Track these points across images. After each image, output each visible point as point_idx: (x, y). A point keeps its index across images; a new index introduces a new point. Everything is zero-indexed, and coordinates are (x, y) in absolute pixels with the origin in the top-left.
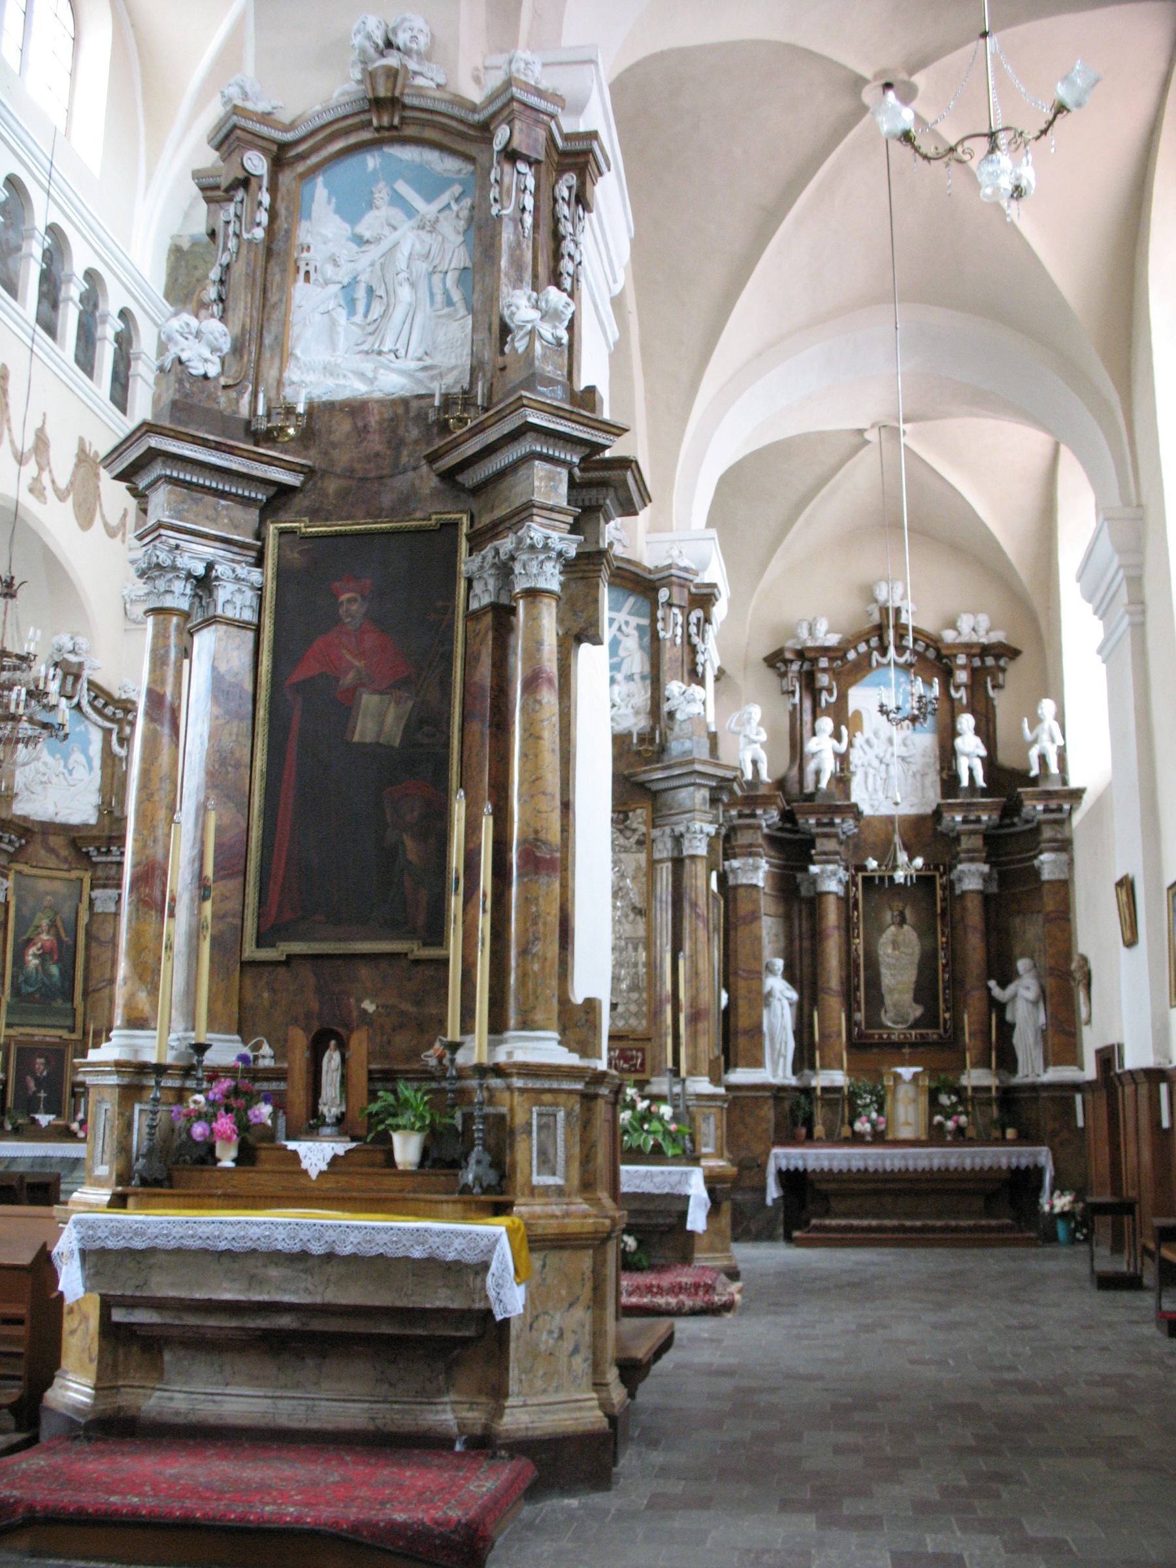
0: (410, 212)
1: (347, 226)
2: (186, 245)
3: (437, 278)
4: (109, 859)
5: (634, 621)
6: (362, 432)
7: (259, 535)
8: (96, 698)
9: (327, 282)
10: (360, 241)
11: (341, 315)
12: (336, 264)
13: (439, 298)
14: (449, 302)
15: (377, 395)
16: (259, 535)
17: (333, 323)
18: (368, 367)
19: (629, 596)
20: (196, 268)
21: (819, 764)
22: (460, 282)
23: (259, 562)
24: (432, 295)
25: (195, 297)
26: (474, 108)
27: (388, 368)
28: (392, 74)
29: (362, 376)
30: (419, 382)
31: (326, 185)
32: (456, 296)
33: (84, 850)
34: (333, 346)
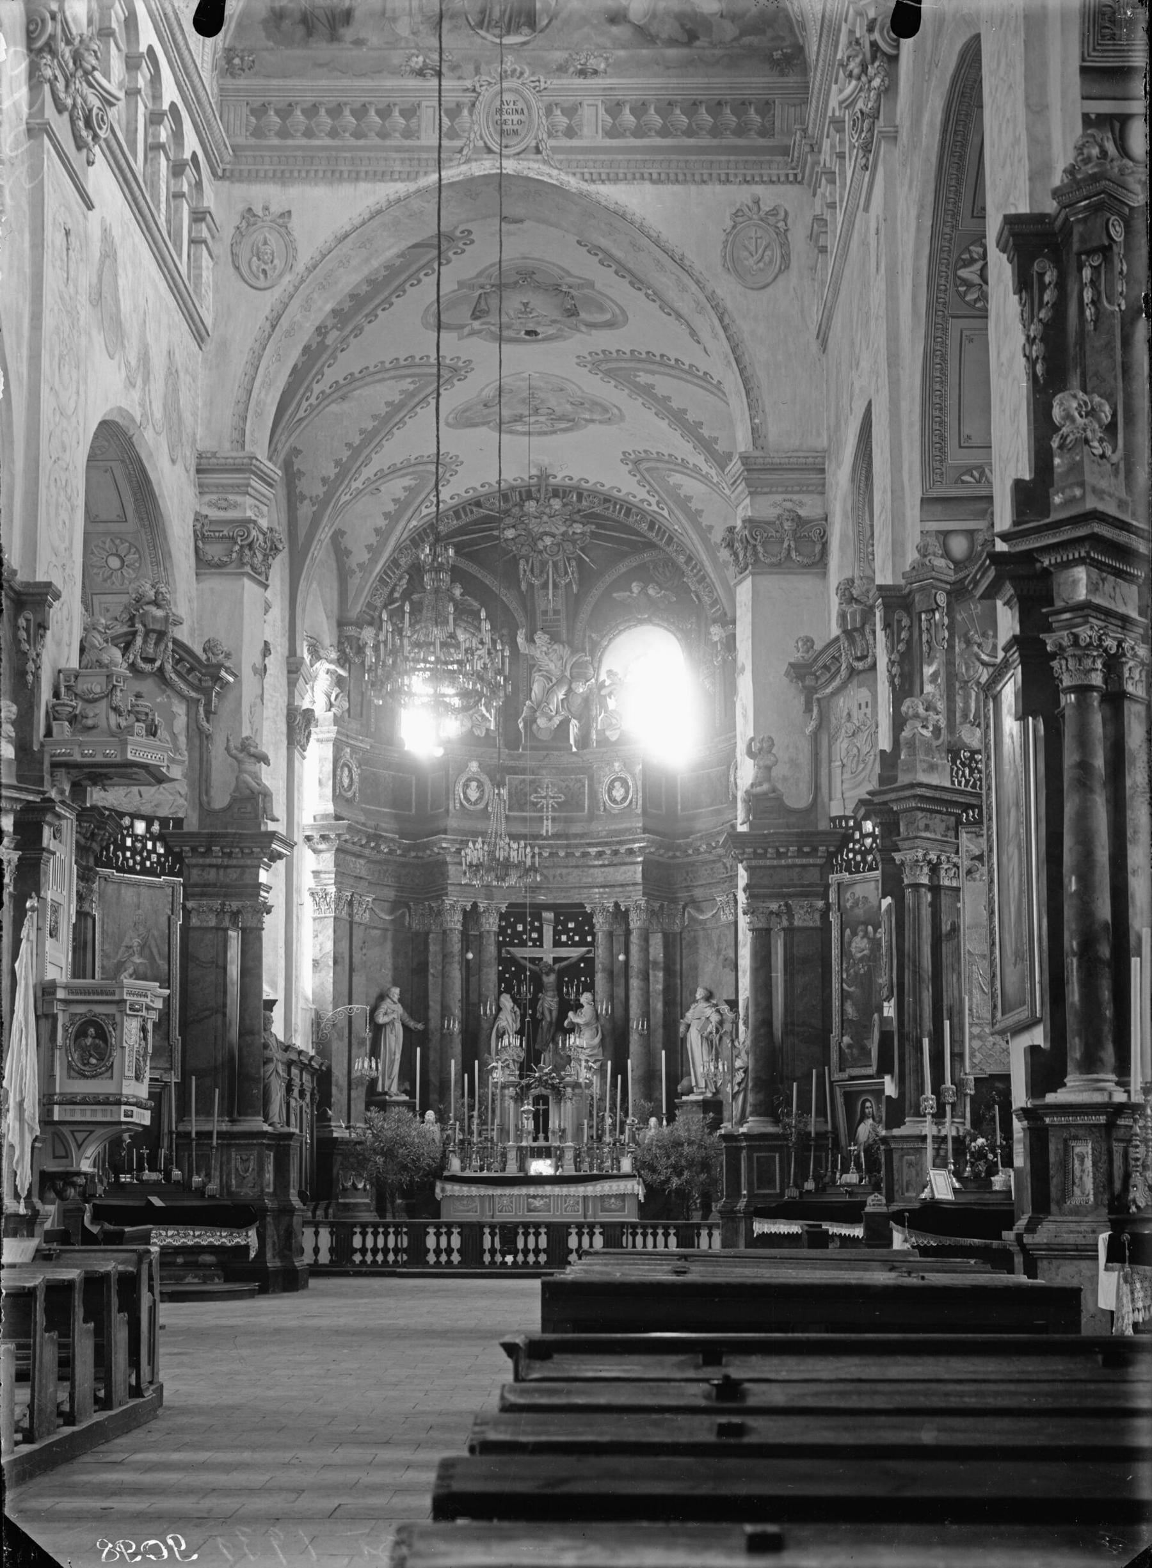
4: (208, 861)
8: (181, 660)
33: (177, 850)
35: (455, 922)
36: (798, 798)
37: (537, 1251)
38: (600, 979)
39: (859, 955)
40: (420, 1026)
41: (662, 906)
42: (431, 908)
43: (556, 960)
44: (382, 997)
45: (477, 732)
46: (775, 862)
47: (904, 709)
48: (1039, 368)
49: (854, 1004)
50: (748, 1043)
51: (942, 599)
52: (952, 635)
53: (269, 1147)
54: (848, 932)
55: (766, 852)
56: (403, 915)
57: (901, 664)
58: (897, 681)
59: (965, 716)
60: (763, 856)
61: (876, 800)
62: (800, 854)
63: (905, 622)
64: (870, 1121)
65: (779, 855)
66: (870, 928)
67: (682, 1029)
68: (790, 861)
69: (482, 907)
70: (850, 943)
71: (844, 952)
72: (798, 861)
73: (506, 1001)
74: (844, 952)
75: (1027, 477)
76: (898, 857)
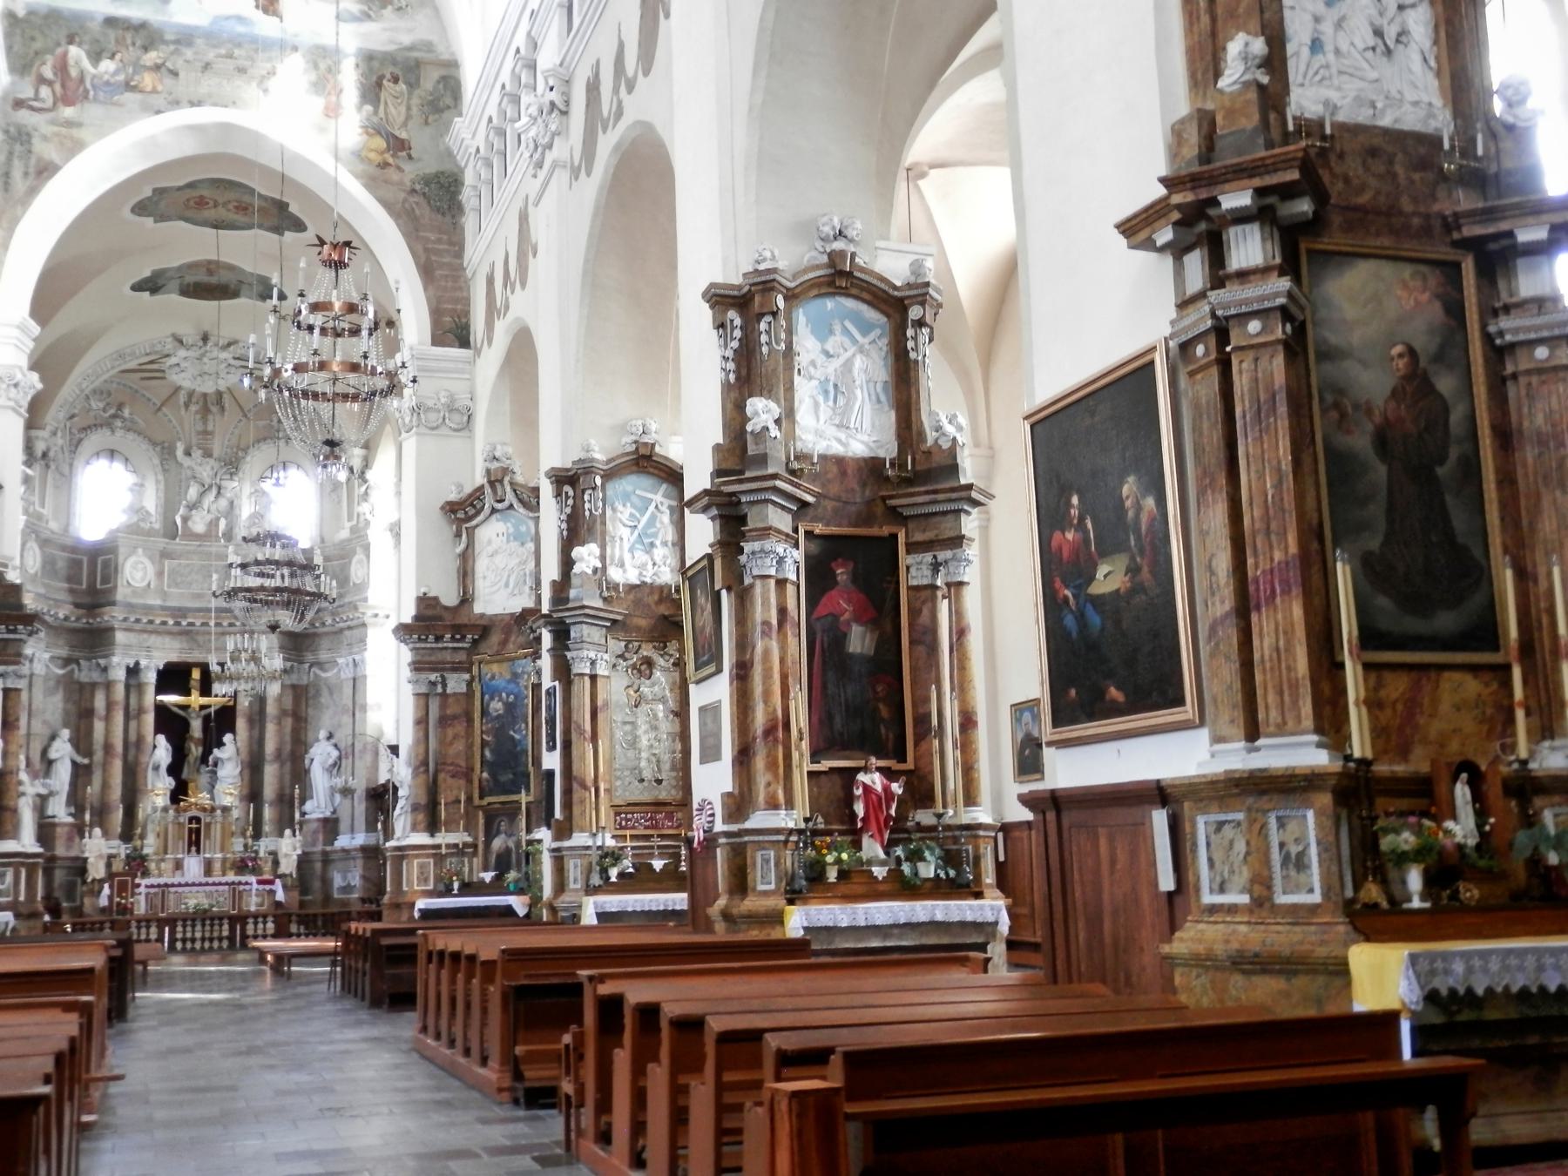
0: (854, 341)
1: (819, 344)
2: (21, 13)
3: (871, 385)
5: (667, 502)
7: (796, 530)
9: (811, 378)
10: (828, 355)
11: (821, 399)
12: (815, 367)
13: (873, 397)
14: (879, 401)
15: (850, 454)
16: (796, 530)
18: (843, 436)
20: (33, 39)
21: (455, 546)
22: (885, 389)
23: (796, 546)
25: (35, 69)
26: (895, 288)
28: (842, 254)
29: (839, 441)
30: (871, 449)
31: (805, 314)
32: (883, 398)
34: (818, 420)
35: (119, 675)
36: (450, 598)
37: (220, 939)
38: (241, 724)
39: (495, 714)
40: (86, 761)
41: (292, 667)
42: (98, 665)
43: (203, 707)
44: (53, 737)
45: (142, 525)
46: (434, 645)
47: (574, 554)
48: (732, 377)
49: (492, 751)
50: (410, 777)
51: (598, 481)
52: (604, 505)
53: (23, 864)
54: (487, 697)
56: (72, 671)
57: (567, 522)
58: (565, 533)
60: (425, 641)
61: (555, 615)
62: (453, 639)
63: (571, 493)
64: (503, 836)
65: (438, 639)
66: (504, 695)
67: (307, 762)
69: (143, 663)
70: (488, 705)
71: (484, 712)
72: (451, 645)
73: (161, 739)
74: (484, 712)
75: (721, 441)
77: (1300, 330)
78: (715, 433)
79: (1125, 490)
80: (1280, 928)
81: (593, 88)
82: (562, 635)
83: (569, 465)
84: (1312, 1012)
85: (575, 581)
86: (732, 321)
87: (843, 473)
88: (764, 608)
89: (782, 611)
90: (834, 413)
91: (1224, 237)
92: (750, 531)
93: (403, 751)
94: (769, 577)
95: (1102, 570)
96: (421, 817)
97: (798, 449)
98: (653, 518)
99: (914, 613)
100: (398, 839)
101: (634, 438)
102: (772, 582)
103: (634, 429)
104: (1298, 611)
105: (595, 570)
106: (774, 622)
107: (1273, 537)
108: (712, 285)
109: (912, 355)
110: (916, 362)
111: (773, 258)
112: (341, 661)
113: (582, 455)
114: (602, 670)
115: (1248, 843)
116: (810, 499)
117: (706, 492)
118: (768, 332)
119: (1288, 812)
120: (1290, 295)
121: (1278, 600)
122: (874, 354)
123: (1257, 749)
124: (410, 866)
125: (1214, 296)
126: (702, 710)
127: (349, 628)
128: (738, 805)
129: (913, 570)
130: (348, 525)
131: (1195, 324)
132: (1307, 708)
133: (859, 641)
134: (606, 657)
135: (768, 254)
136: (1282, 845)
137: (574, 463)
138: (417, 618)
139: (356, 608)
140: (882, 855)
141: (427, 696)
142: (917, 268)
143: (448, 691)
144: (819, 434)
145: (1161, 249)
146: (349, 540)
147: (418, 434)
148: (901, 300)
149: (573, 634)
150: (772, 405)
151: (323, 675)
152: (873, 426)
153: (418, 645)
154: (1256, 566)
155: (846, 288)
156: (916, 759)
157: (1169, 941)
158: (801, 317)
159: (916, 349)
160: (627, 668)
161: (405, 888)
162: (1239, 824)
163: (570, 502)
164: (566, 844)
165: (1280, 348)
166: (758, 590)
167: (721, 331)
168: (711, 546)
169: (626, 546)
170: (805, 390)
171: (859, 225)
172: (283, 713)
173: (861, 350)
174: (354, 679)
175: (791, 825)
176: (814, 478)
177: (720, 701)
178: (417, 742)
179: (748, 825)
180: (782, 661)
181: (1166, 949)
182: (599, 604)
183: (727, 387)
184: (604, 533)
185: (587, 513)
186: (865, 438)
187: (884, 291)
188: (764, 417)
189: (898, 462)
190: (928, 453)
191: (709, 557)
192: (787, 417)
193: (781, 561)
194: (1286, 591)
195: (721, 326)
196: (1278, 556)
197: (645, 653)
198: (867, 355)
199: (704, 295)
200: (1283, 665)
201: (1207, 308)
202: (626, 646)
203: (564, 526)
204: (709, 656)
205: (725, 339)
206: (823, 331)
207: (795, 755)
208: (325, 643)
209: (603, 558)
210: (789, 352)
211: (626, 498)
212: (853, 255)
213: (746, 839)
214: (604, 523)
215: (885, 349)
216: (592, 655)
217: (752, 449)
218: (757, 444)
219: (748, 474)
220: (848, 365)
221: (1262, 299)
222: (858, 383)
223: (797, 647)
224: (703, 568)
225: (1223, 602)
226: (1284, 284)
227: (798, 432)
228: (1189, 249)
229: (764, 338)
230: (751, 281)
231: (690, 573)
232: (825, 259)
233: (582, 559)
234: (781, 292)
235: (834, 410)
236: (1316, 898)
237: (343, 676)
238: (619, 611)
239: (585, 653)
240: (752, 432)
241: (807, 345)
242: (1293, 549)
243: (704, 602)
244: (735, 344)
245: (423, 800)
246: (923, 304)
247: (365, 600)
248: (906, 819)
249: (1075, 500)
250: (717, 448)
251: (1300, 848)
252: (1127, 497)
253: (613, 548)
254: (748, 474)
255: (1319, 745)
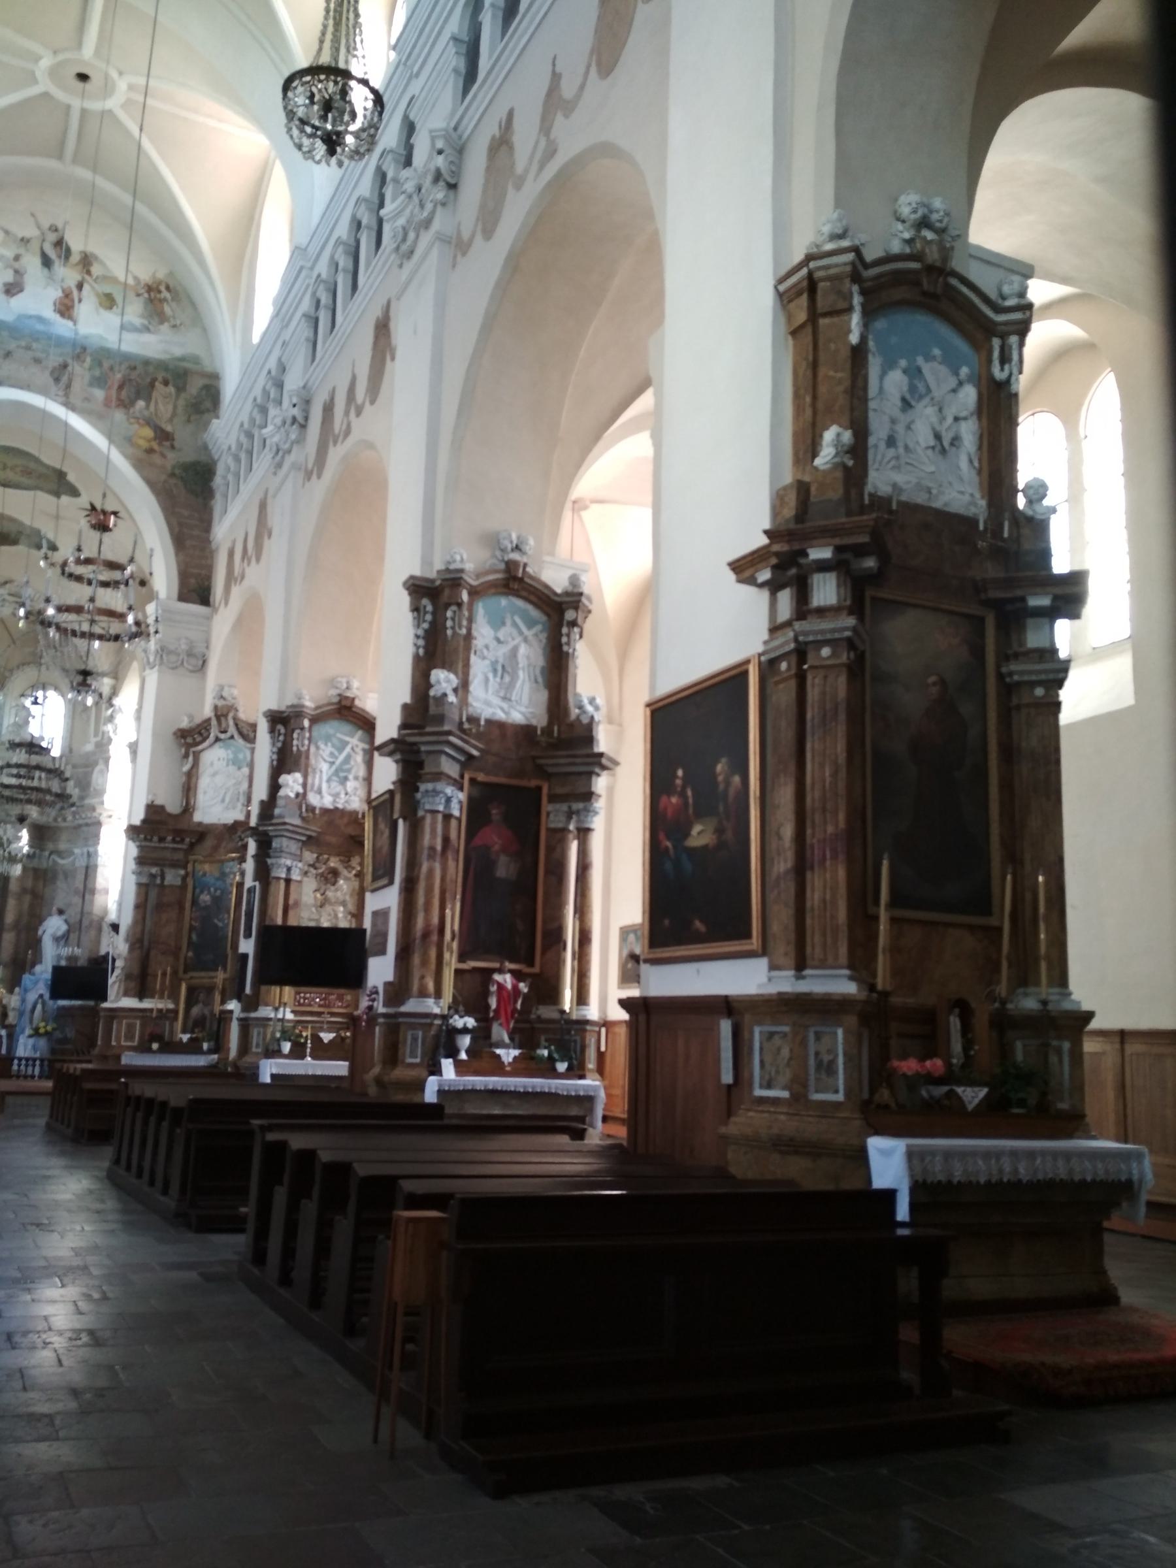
0: (521, 633)
3: (531, 669)
6: (503, 736)
7: (462, 777)
9: (484, 658)
10: (498, 641)
11: (491, 676)
15: (510, 721)
16: (462, 777)
17: (487, 680)
18: (505, 705)
19: (357, 731)
23: (461, 789)
24: (529, 676)
26: (555, 594)
27: (516, 710)
29: (502, 709)
30: (527, 718)
32: (540, 679)
34: (487, 690)
36: (173, 806)
39: (203, 905)
41: (34, 853)
46: (157, 845)
48: (421, 651)
51: (306, 723)
54: (198, 891)
55: (152, 837)
58: (275, 763)
59: (313, 785)
60: (151, 840)
61: (261, 828)
62: (174, 841)
63: (283, 731)
65: (162, 840)
66: (212, 889)
67: (40, 932)
68: (167, 845)
70: (199, 896)
71: (195, 902)
72: (171, 845)
74: (195, 902)
76: (269, 861)
77: (861, 657)
78: (405, 695)
79: (719, 768)
80: (810, 1119)
81: (328, 409)
82: (265, 845)
83: (283, 708)
84: (830, 1187)
85: (280, 802)
86: (425, 607)
87: (503, 736)
88: (431, 837)
89: (446, 840)
90: (501, 688)
91: (809, 581)
92: (428, 774)
93: (123, 929)
94: (438, 812)
95: (697, 829)
96: (132, 985)
97: (470, 713)
98: (348, 759)
99: (550, 849)
100: (112, 1002)
101: (338, 691)
102: (440, 817)
103: (339, 685)
104: (842, 873)
105: (297, 795)
106: (439, 848)
107: (828, 815)
108: (412, 577)
109: (565, 648)
110: (567, 654)
111: (462, 560)
112: (77, 851)
113: (295, 701)
114: (295, 876)
115: (791, 1051)
116: (475, 753)
117: (393, 741)
118: (453, 619)
119: (823, 1029)
120: (854, 629)
121: (828, 863)
122: (535, 643)
123: (803, 978)
124: (120, 1024)
125: (797, 625)
126: (375, 914)
127: (87, 825)
128: (398, 991)
129: (552, 817)
130: (93, 740)
131: (782, 646)
132: (843, 950)
133: (504, 869)
134: (300, 865)
135: (458, 558)
136: (817, 1054)
137: (288, 707)
138: (144, 821)
139: (94, 809)
140: (506, 1039)
141: (147, 885)
142: (574, 580)
143: (166, 883)
144: (488, 703)
145: (761, 586)
146: (93, 753)
147: (160, 671)
148: (560, 604)
149: (274, 845)
150: (452, 676)
151: (61, 861)
152: (530, 700)
153: (144, 844)
154: (813, 835)
155: (518, 590)
156: (541, 968)
157: (726, 1124)
158: (480, 609)
159: (568, 644)
160: (317, 875)
161: (114, 1043)
162: (785, 1035)
163: (281, 738)
164: (253, 1015)
165: (844, 669)
166: (428, 819)
167: (415, 613)
168: (394, 783)
169: (325, 778)
170: (479, 667)
171: (531, 542)
172: (24, 891)
173: (526, 640)
174: (87, 868)
175: (437, 1010)
176: (479, 736)
177: (389, 908)
178: (135, 922)
179: (403, 1009)
180: (443, 879)
181: (723, 1130)
182: (297, 821)
183: (417, 659)
184: (307, 766)
185: (295, 749)
186: (523, 709)
187: (548, 597)
188: (444, 685)
189: (547, 731)
190: (571, 726)
191: (391, 793)
192: (463, 687)
193: (448, 800)
194: (834, 857)
195: (416, 609)
196: (830, 829)
197: (332, 865)
198: (531, 645)
199: (405, 584)
200: (828, 914)
201: (791, 634)
202: (317, 858)
203: (275, 757)
204: (383, 873)
205: (418, 622)
206: (497, 622)
207: (447, 955)
208: (64, 836)
209: (304, 785)
210: (469, 637)
211: (328, 739)
212: (525, 565)
213: (401, 1020)
214: (307, 757)
215: (544, 641)
216: (289, 862)
217: (433, 710)
218: (437, 706)
219: (429, 729)
220: (514, 652)
221: (833, 631)
222: (521, 665)
223: (456, 869)
224: (384, 802)
225: (786, 861)
226: (851, 621)
227: (470, 699)
228: (781, 587)
229: (449, 623)
230: (443, 577)
231: (374, 804)
232: (502, 566)
233: (287, 785)
234: (467, 589)
235: (500, 684)
236: (840, 1097)
237: (77, 864)
238: (314, 829)
239: (283, 861)
240: (434, 697)
241: (483, 633)
242: (842, 824)
243: (383, 827)
244: (426, 626)
245: (136, 971)
246: (576, 608)
247: (102, 803)
248: (530, 1012)
249: (680, 773)
250: (405, 707)
251: (831, 1057)
252: (720, 774)
253: (314, 778)
254: (429, 729)
255: (851, 978)
